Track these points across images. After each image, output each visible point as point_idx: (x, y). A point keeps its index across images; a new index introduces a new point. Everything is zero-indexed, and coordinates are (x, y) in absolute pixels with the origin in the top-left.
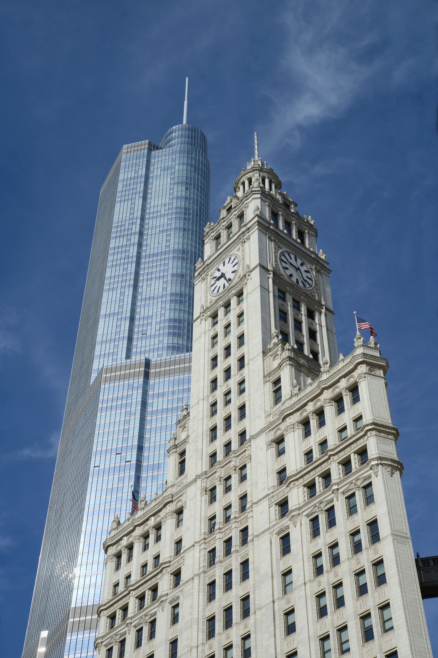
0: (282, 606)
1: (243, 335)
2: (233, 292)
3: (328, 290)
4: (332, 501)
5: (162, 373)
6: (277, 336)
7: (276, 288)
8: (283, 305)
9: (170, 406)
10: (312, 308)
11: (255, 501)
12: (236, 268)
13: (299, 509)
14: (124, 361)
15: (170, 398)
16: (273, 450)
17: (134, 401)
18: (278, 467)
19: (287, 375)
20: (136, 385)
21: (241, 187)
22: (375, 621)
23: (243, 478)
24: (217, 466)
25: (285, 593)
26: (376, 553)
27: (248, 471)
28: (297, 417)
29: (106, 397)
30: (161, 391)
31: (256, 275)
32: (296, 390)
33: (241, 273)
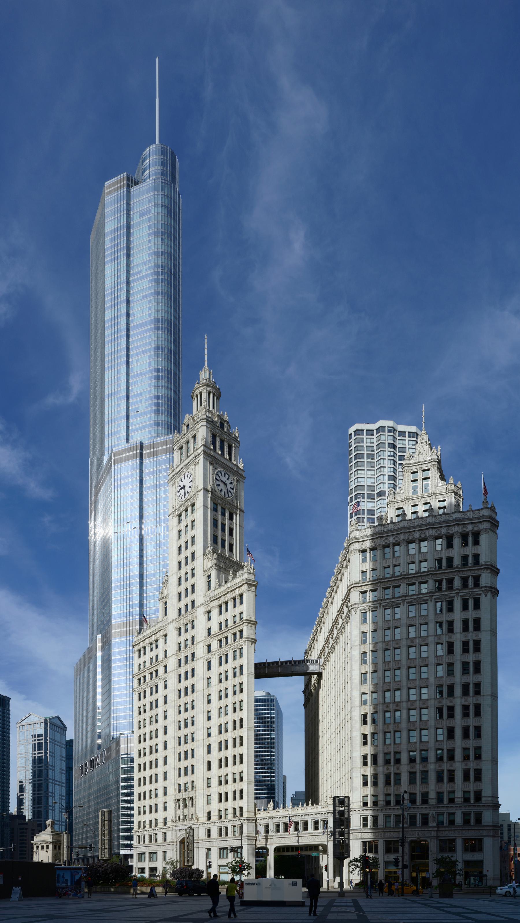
0: (206, 692)
1: (194, 537)
2: (190, 502)
3: (243, 494)
4: (227, 651)
5: (152, 454)
6: (211, 546)
7: (212, 503)
8: (215, 515)
9: (158, 483)
10: (232, 511)
11: (198, 641)
12: (191, 484)
13: (215, 651)
14: (126, 445)
15: (158, 476)
16: (206, 617)
17: (135, 479)
18: (208, 627)
19: (214, 573)
20: (135, 466)
21: (196, 398)
22: (237, 706)
23: (193, 627)
24: (181, 617)
25: (208, 687)
26: (241, 679)
27: (195, 623)
28: (216, 603)
29: (116, 477)
30: (152, 470)
31: (201, 494)
32: (217, 587)
33: (194, 489)
